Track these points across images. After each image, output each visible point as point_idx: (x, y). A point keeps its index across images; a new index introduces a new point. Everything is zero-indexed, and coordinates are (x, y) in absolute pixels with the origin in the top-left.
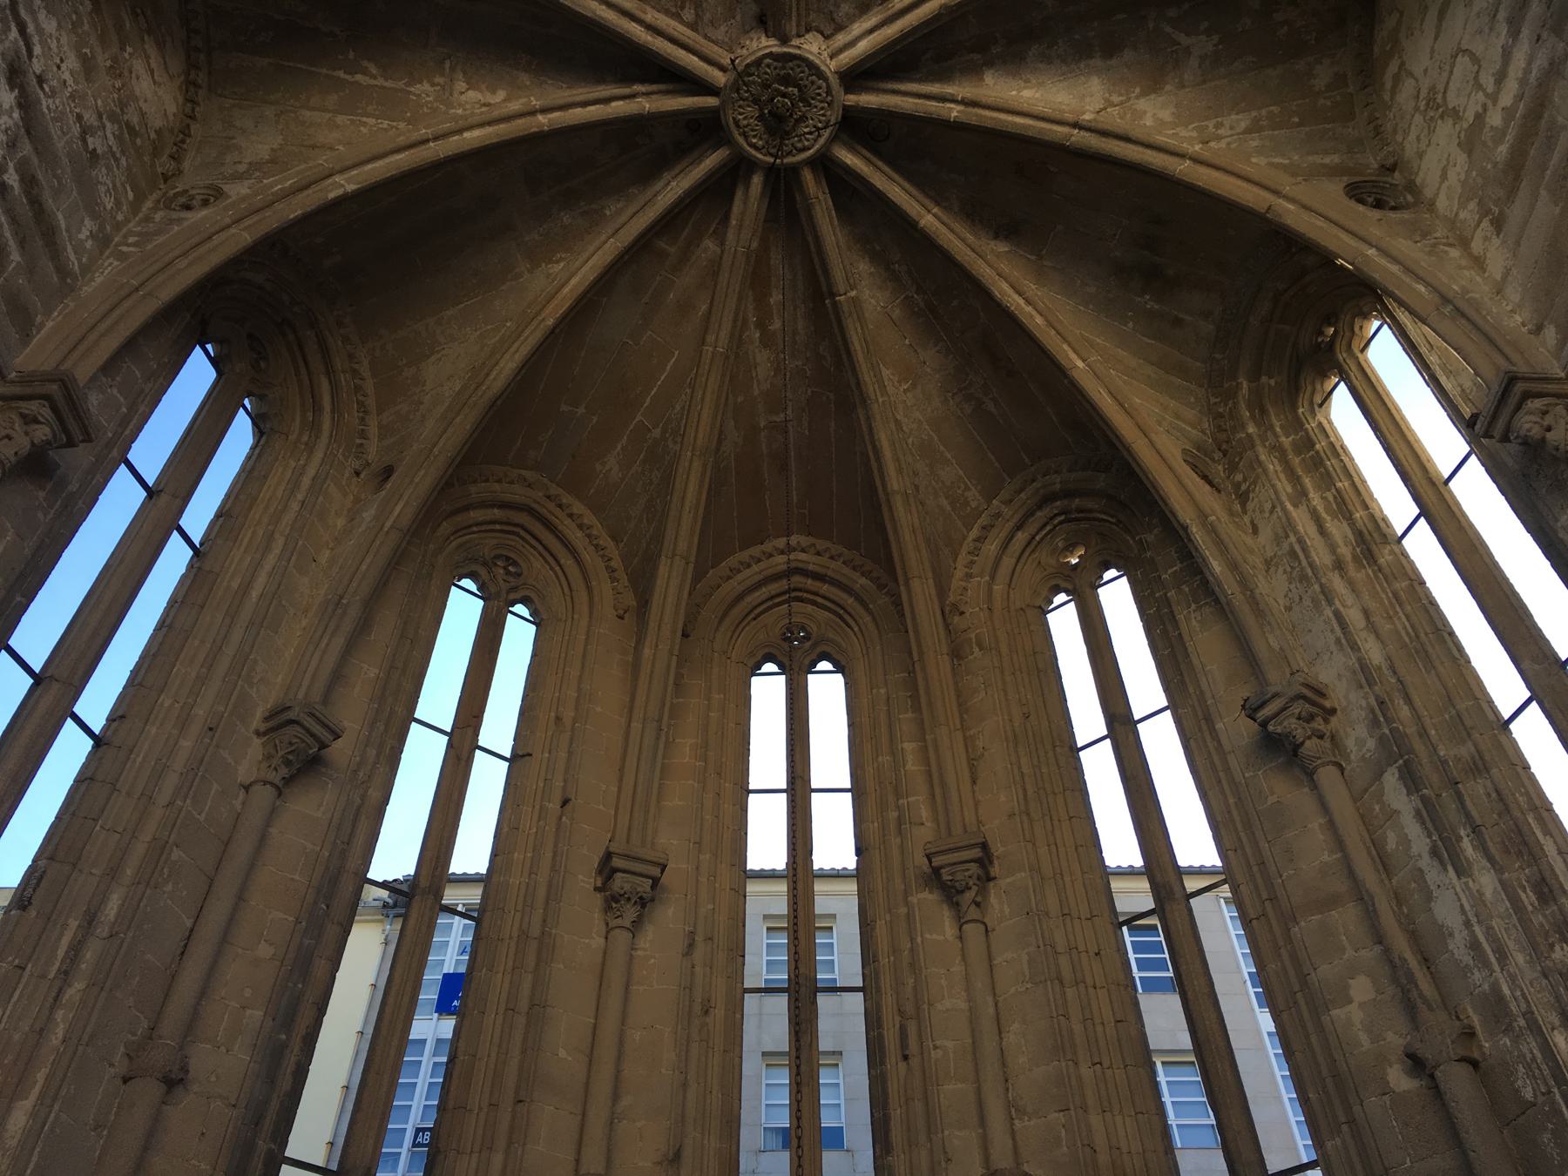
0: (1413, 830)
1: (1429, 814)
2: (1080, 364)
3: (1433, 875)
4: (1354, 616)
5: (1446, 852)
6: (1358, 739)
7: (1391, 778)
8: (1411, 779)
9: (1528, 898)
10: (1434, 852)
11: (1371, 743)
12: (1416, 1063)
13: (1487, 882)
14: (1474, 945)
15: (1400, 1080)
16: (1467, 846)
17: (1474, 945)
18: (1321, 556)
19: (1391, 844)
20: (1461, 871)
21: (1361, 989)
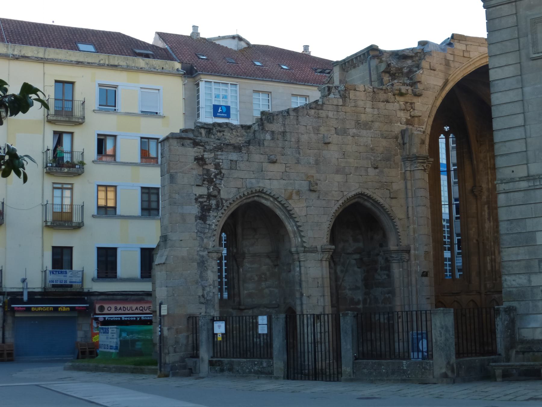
0: (486, 214)
1: (489, 214)
2: (468, 119)
3: (487, 220)
4: (490, 178)
5: (489, 219)
6: (484, 198)
7: (486, 206)
8: (489, 208)
9: (495, 227)
10: (488, 218)
11: (485, 200)
12: (477, 240)
13: (492, 223)
14: (488, 231)
15: (475, 241)
16: (491, 218)
17: (488, 231)
18: (489, 166)
19: (483, 214)
20: (490, 222)
21: (474, 229)
